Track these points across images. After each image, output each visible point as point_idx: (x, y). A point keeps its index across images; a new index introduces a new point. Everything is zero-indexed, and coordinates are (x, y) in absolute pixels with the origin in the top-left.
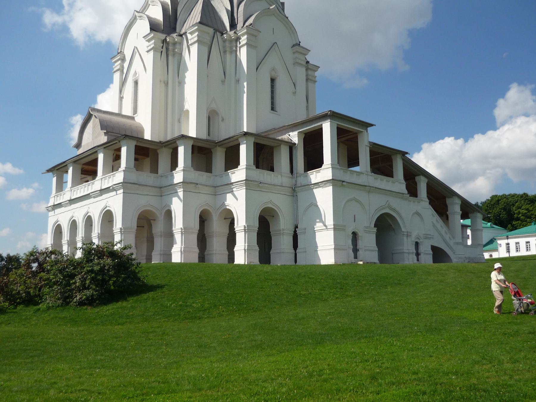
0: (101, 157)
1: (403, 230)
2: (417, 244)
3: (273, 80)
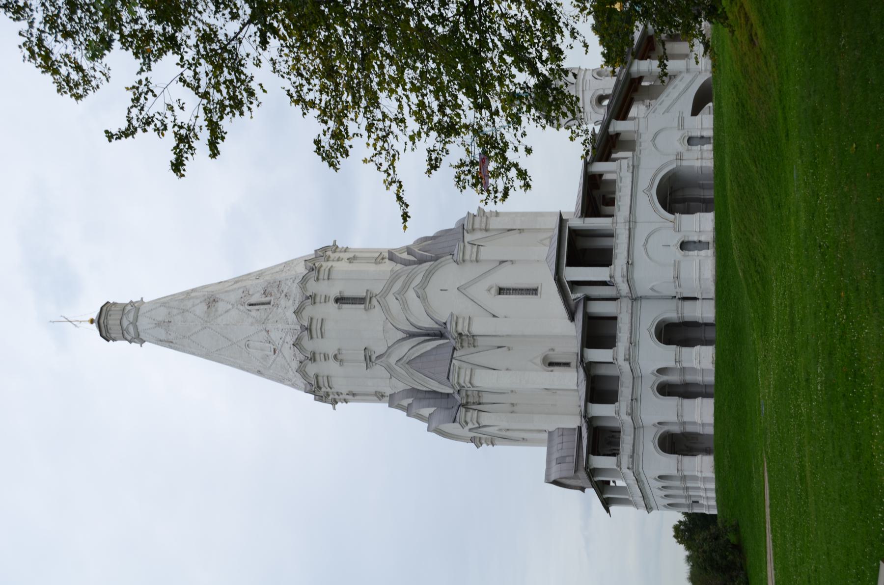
1: (674, 166)
2: (691, 141)
3: (501, 291)
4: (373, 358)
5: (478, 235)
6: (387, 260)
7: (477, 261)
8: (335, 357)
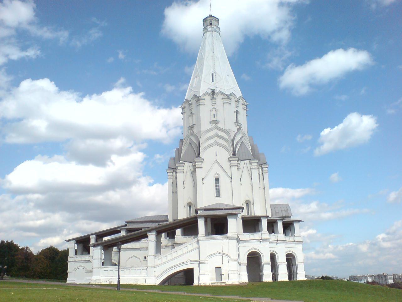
3: (217, 179)
5: (249, 166)
6: (238, 127)
7: (231, 166)
8: (192, 113)
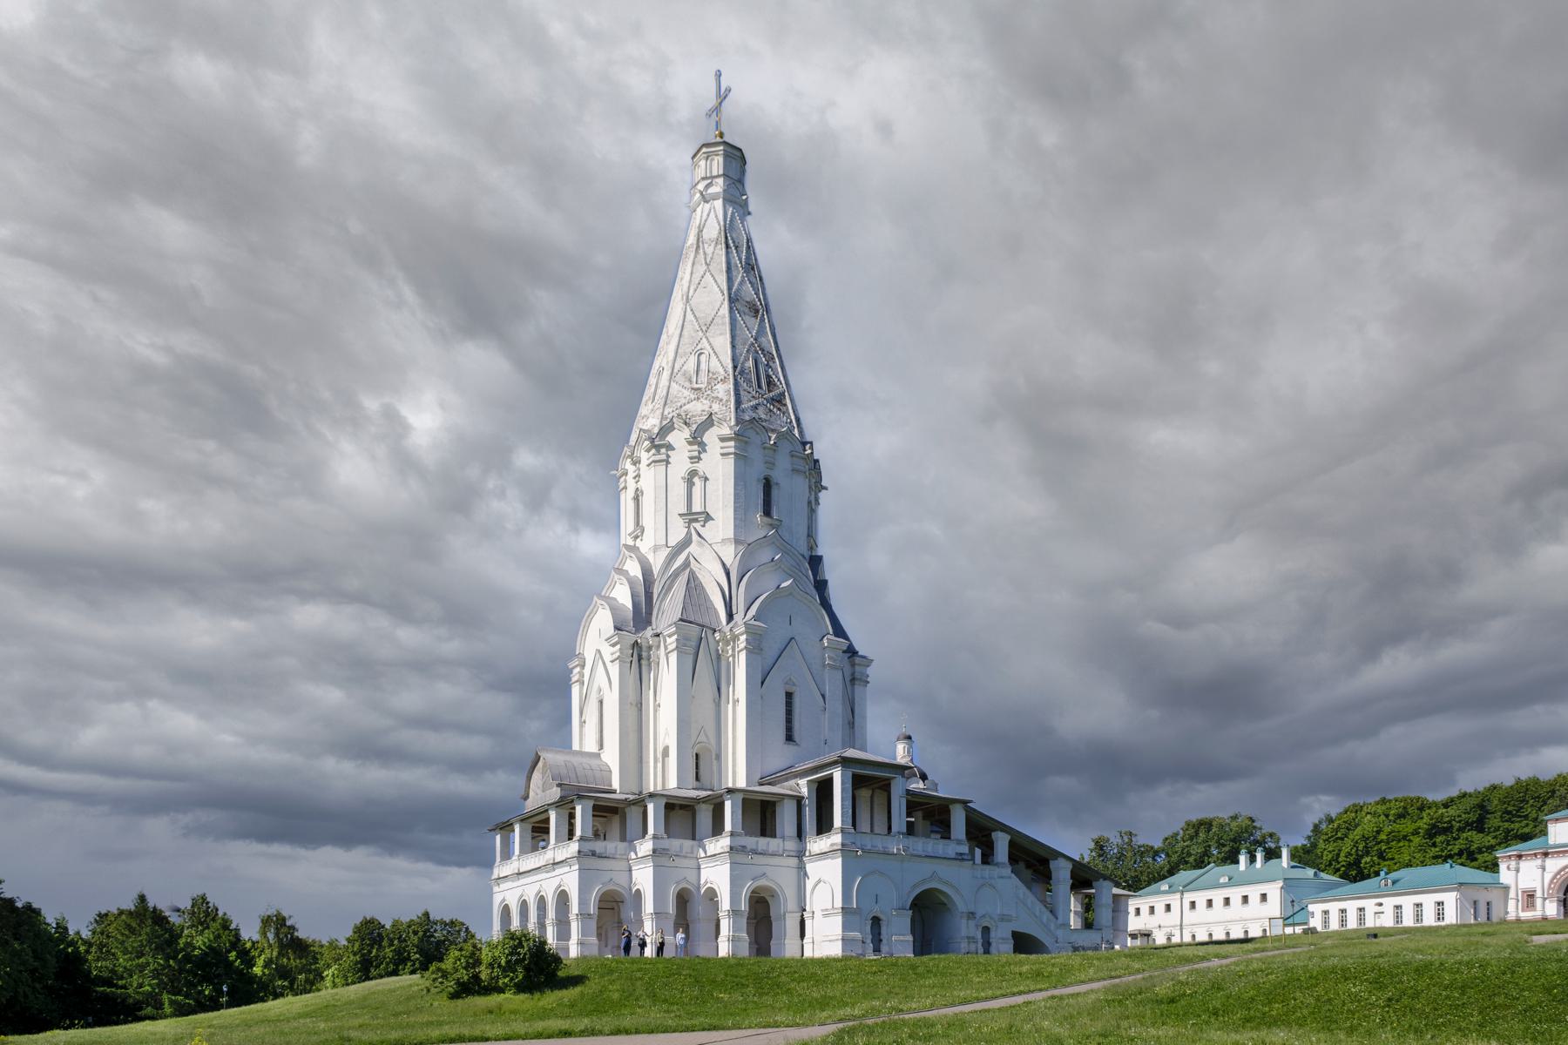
0: (553, 816)
3: (789, 695)
4: (697, 525)
